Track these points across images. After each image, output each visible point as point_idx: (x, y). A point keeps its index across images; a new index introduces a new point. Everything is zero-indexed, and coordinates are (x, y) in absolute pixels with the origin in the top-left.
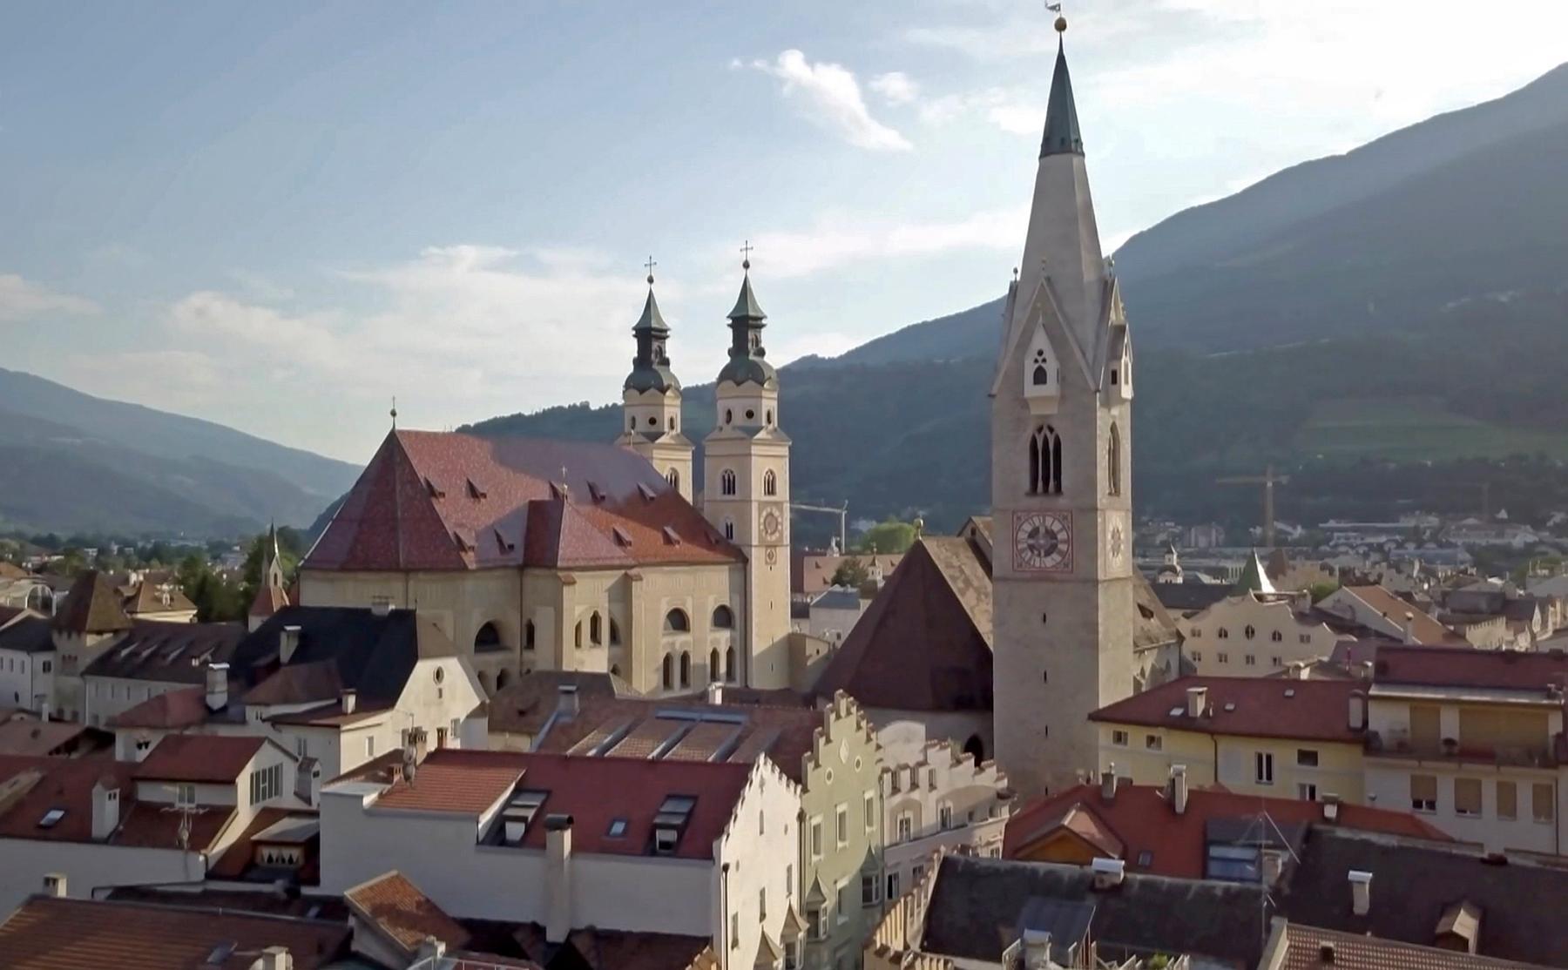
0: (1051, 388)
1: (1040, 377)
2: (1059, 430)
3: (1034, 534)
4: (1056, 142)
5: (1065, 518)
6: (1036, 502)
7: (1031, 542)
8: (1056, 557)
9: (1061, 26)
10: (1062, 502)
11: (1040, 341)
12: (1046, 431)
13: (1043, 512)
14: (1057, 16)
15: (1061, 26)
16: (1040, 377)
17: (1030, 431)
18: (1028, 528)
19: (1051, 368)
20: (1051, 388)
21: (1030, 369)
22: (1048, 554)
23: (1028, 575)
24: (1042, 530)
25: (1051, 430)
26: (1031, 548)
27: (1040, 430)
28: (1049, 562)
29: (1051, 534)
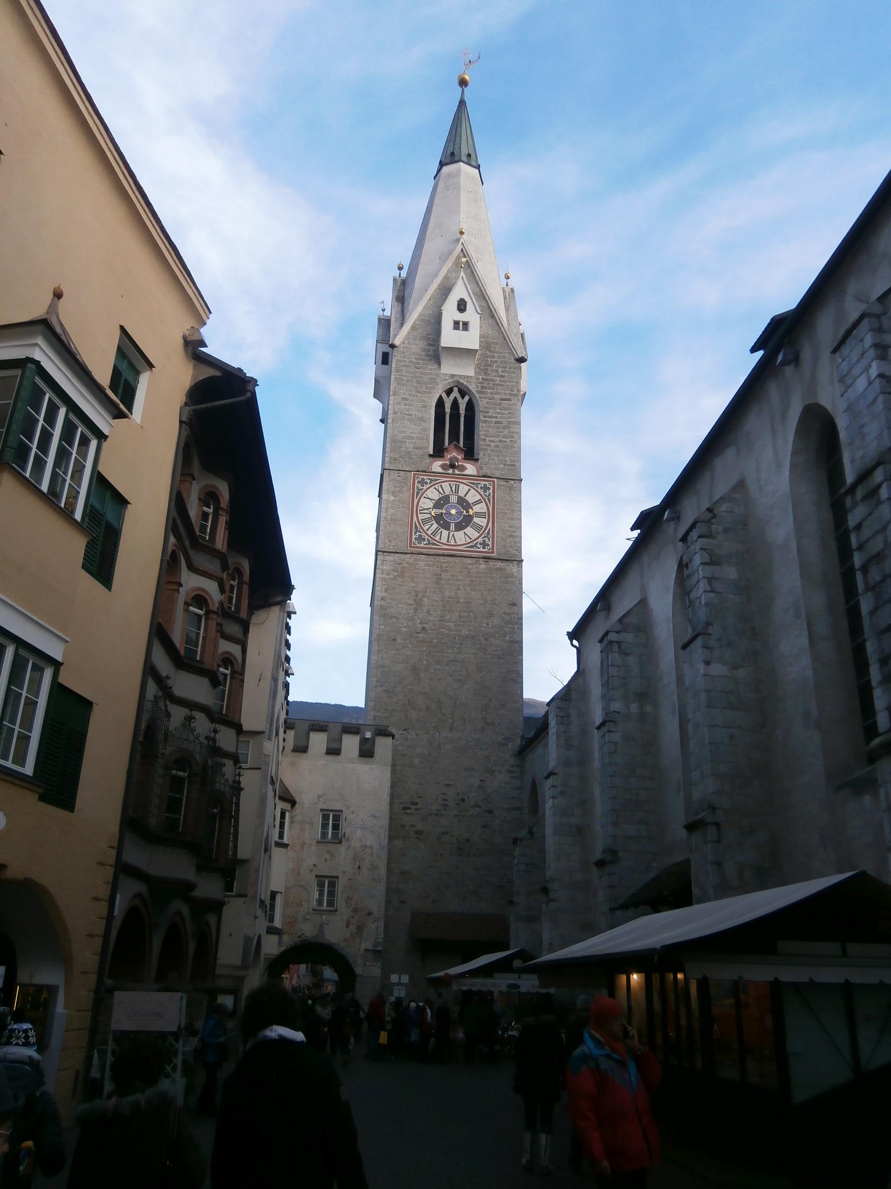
8: (469, 530)
12: (455, 393)
18: (433, 494)
22: (460, 527)
24: (454, 499)
26: (438, 518)
27: (449, 392)
28: (460, 537)
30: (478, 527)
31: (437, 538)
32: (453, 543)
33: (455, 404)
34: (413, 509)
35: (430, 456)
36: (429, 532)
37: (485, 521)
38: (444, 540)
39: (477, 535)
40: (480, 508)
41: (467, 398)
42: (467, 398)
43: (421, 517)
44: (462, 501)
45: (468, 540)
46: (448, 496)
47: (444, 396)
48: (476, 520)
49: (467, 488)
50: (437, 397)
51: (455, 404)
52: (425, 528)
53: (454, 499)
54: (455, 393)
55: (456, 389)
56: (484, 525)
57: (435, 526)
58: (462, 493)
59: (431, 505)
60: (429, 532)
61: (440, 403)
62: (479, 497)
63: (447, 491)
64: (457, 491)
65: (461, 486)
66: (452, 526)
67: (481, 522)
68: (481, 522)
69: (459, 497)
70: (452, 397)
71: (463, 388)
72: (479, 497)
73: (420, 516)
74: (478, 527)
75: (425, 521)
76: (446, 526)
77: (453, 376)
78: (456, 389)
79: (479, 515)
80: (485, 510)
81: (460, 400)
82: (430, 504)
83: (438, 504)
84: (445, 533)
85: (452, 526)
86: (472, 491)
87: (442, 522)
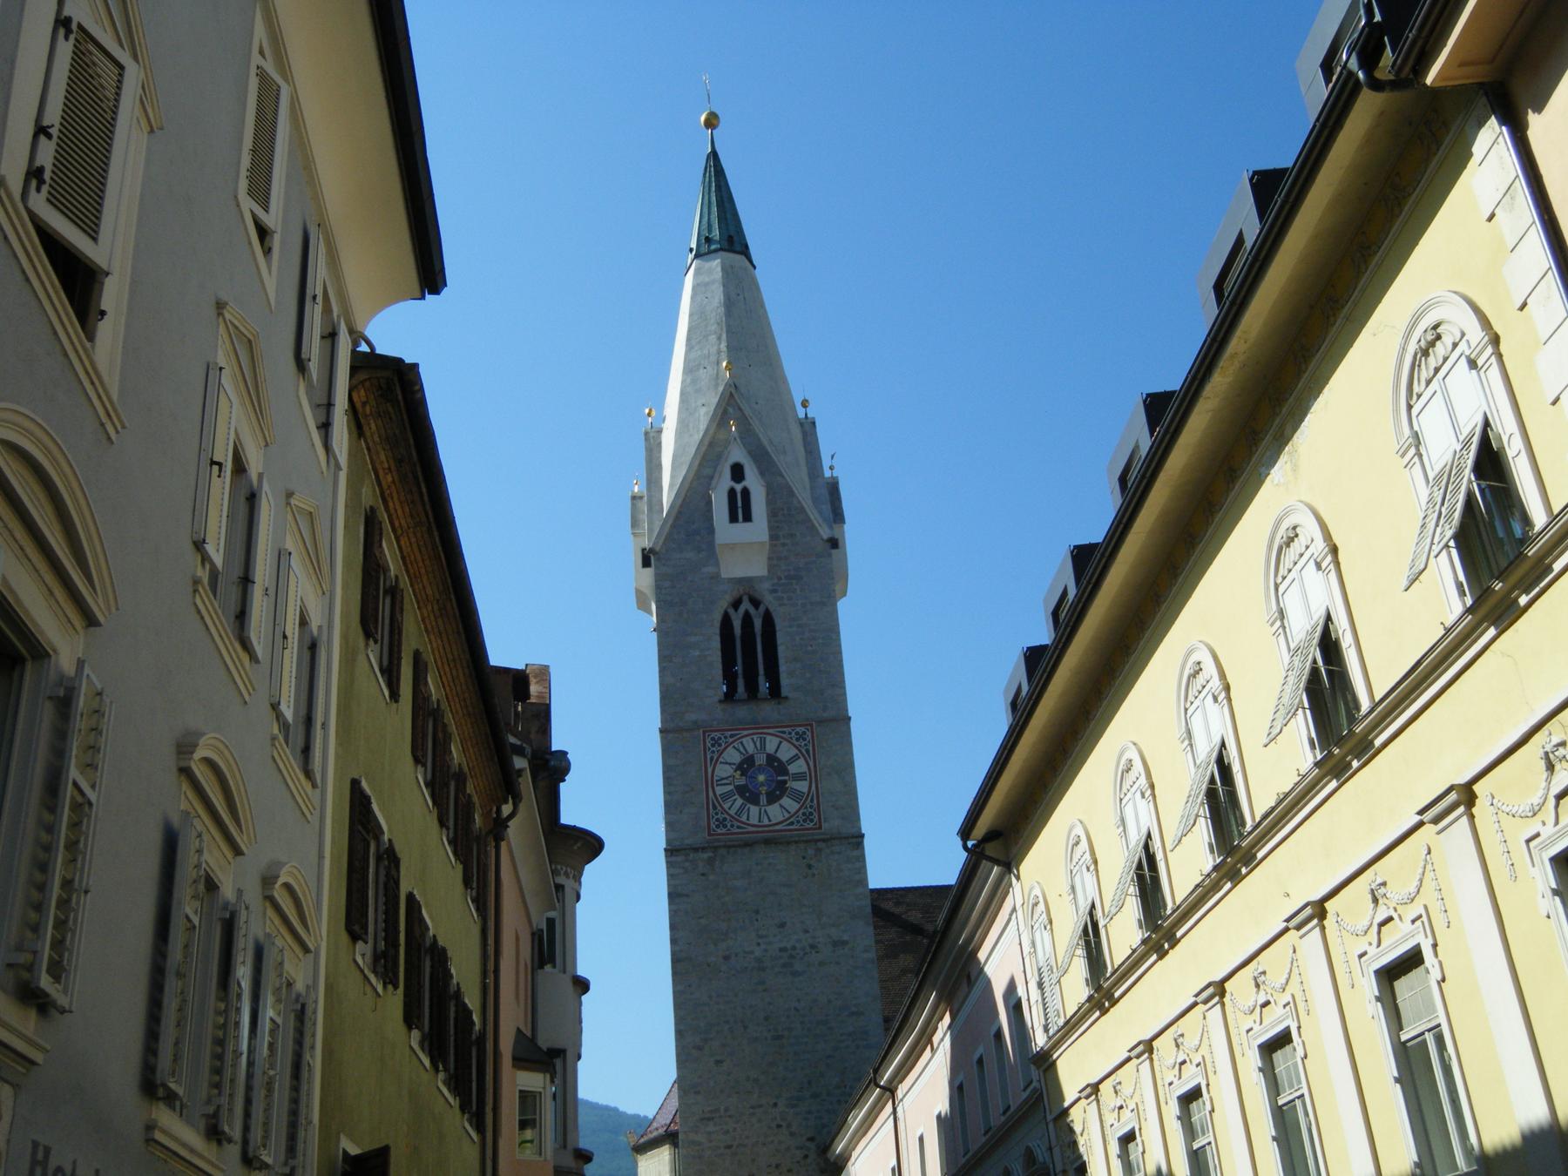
2: (769, 600)
3: (747, 765)
6: (742, 712)
8: (786, 801)
12: (746, 605)
13: (756, 725)
17: (723, 604)
20: (758, 529)
22: (773, 798)
24: (761, 760)
25: (756, 603)
26: (741, 790)
27: (736, 604)
28: (775, 812)
29: (776, 766)
30: (796, 796)
31: (744, 818)
32: (766, 822)
33: (747, 620)
34: (710, 783)
36: (732, 812)
39: (797, 806)
40: (798, 767)
41: (762, 609)
42: (762, 609)
43: (720, 790)
44: (771, 759)
47: (731, 611)
49: (777, 740)
52: (726, 806)
53: (761, 760)
54: (746, 605)
55: (745, 599)
56: (805, 790)
57: (740, 801)
58: (770, 748)
60: (732, 812)
61: (726, 622)
63: (751, 749)
65: (769, 738)
66: (763, 799)
67: (802, 786)
68: (802, 786)
69: (769, 756)
70: (742, 609)
72: (794, 751)
74: (796, 796)
75: (726, 796)
76: (754, 799)
77: (740, 581)
78: (745, 599)
79: (799, 777)
80: (804, 768)
81: (752, 611)
84: (754, 810)
85: (763, 799)
86: (785, 744)
87: (749, 795)
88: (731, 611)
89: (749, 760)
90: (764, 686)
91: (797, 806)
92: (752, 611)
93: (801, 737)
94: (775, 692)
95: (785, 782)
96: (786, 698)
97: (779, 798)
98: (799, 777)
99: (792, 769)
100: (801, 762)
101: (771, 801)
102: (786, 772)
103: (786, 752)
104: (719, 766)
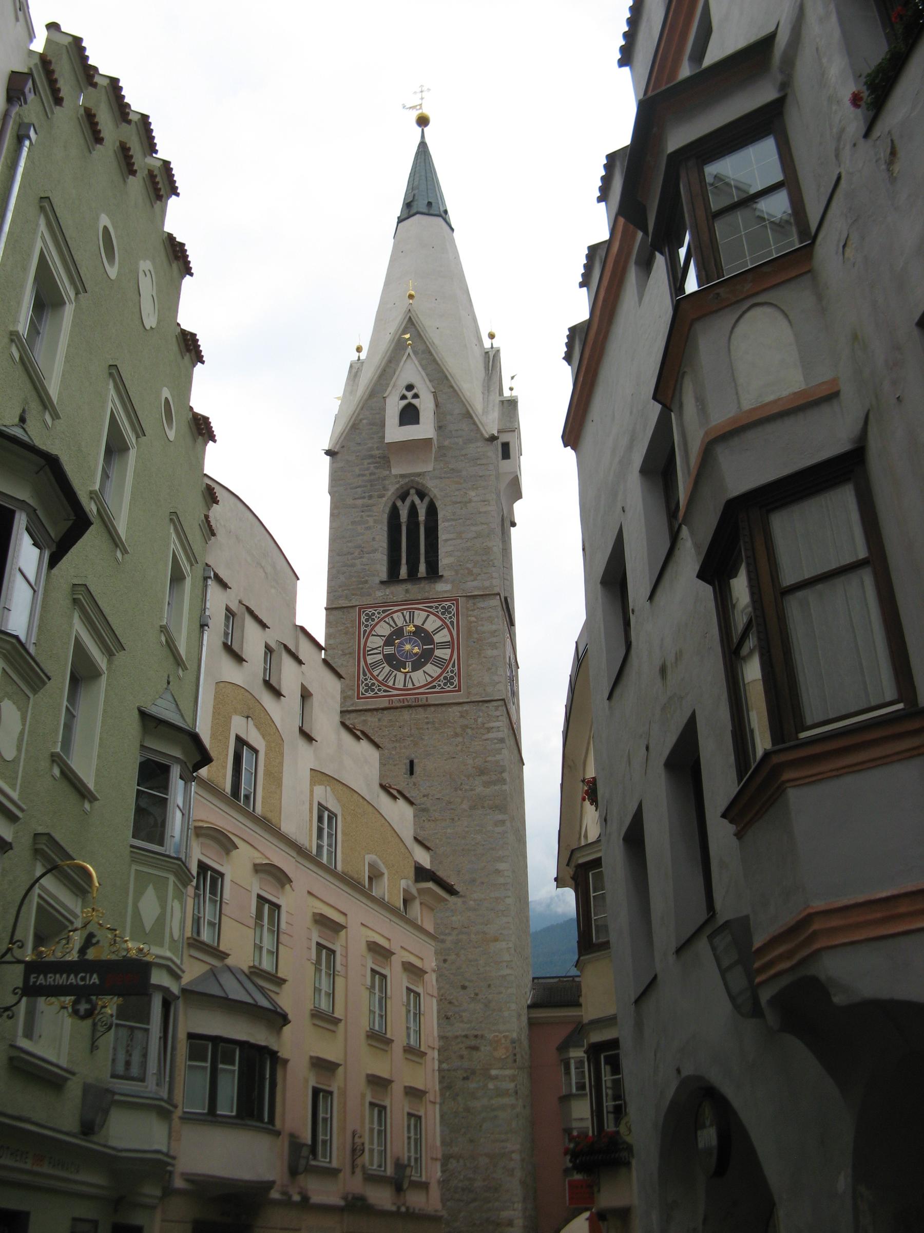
0: (425, 429)
1: (409, 415)
4: (421, 205)
5: (446, 610)
6: (398, 592)
7: (389, 650)
8: (429, 668)
9: (423, 121)
10: (442, 588)
11: (410, 371)
14: (414, 114)
15: (423, 121)
16: (409, 415)
18: (384, 630)
19: (426, 405)
21: (393, 407)
23: (384, 703)
25: (422, 495)
26: (389, 659)
27: (403, 497)
28: (419, 678)
29: (422, 635)
30: (440, 663)
31: (391, 684)
32: (410, 686)
33: (413, 510)
35: (382, 582)
36: (380, 678)
37: (449, 651)
38: (401, 686)
39: (439, 671)
42: (426, 500)
43: (370, 659)
45: (429, 679)
46: (401, 629)
47: (399, 503)
48: (438, 653)
50: (390, 505)
51: (413, 510)
52: (375, 673)
55: (412, 491)
56: (447, 657)
57: (388, 669)
58: (418, 622)
59: (382, 643)
61: (394, 514)
62: (439, 623)
64: (412, 619)
65: (416, 612)
67: (444, 653)
68: (444, 653)
70: (408, 502)
71: (420, 487)
73: (368, 658)
74: (440, 663)
75: (376, 664)
77: (402, 476)
78: (412, 491)
79: (443, 645)
80: (448, 638)
82: (380, 642)
83: (389, 642)
84: (400, 676)
86: (432, 617)
87: (394, 662)
88: (399, 503)
89: (398, 632)
90: (422, 568)
91: (439, 671)
92: (417, 501)
93: (446, 610)
94: (434, 573)
95: (432, 650)
96: (442, 576)
97: (424, 664)
98: (443, 645)
99: (438, 638)
100: (445, 631)
101: (415, 669)
102: (431, 642)
103: (432, 624)
104: (371, 638)
